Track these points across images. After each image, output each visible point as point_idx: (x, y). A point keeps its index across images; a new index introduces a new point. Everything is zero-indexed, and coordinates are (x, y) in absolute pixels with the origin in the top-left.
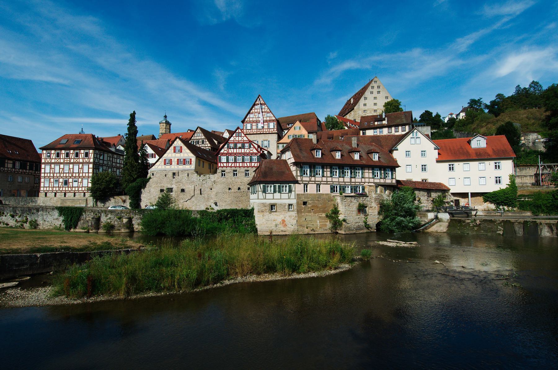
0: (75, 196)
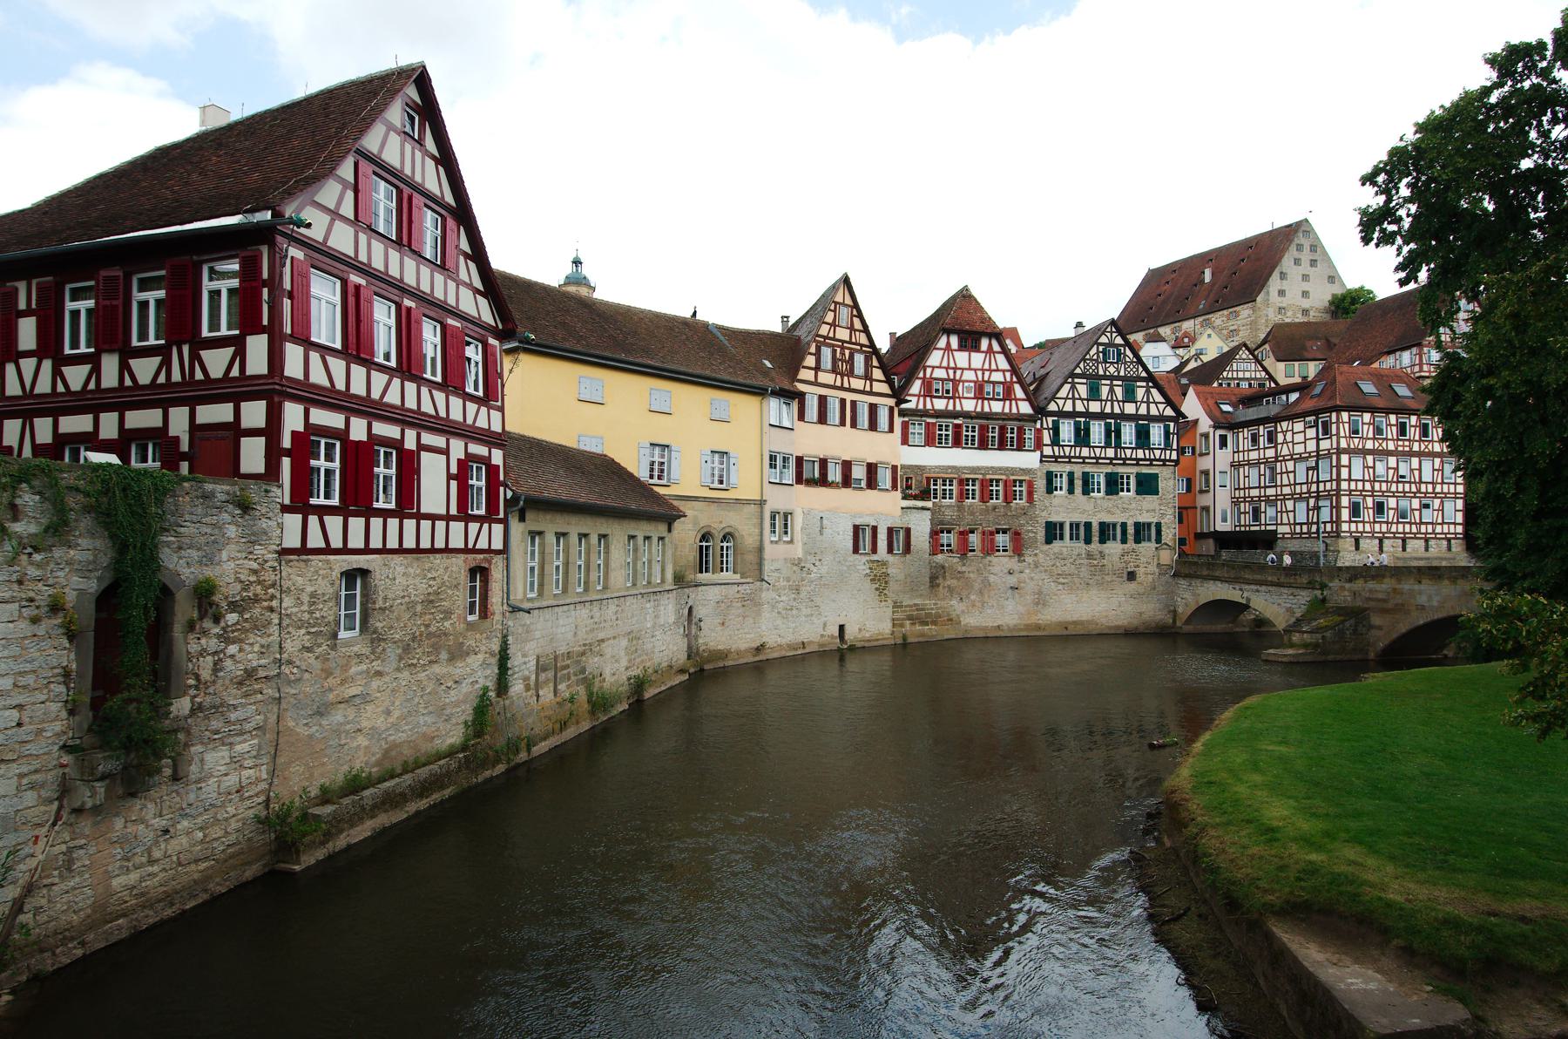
0: (1427, 549)
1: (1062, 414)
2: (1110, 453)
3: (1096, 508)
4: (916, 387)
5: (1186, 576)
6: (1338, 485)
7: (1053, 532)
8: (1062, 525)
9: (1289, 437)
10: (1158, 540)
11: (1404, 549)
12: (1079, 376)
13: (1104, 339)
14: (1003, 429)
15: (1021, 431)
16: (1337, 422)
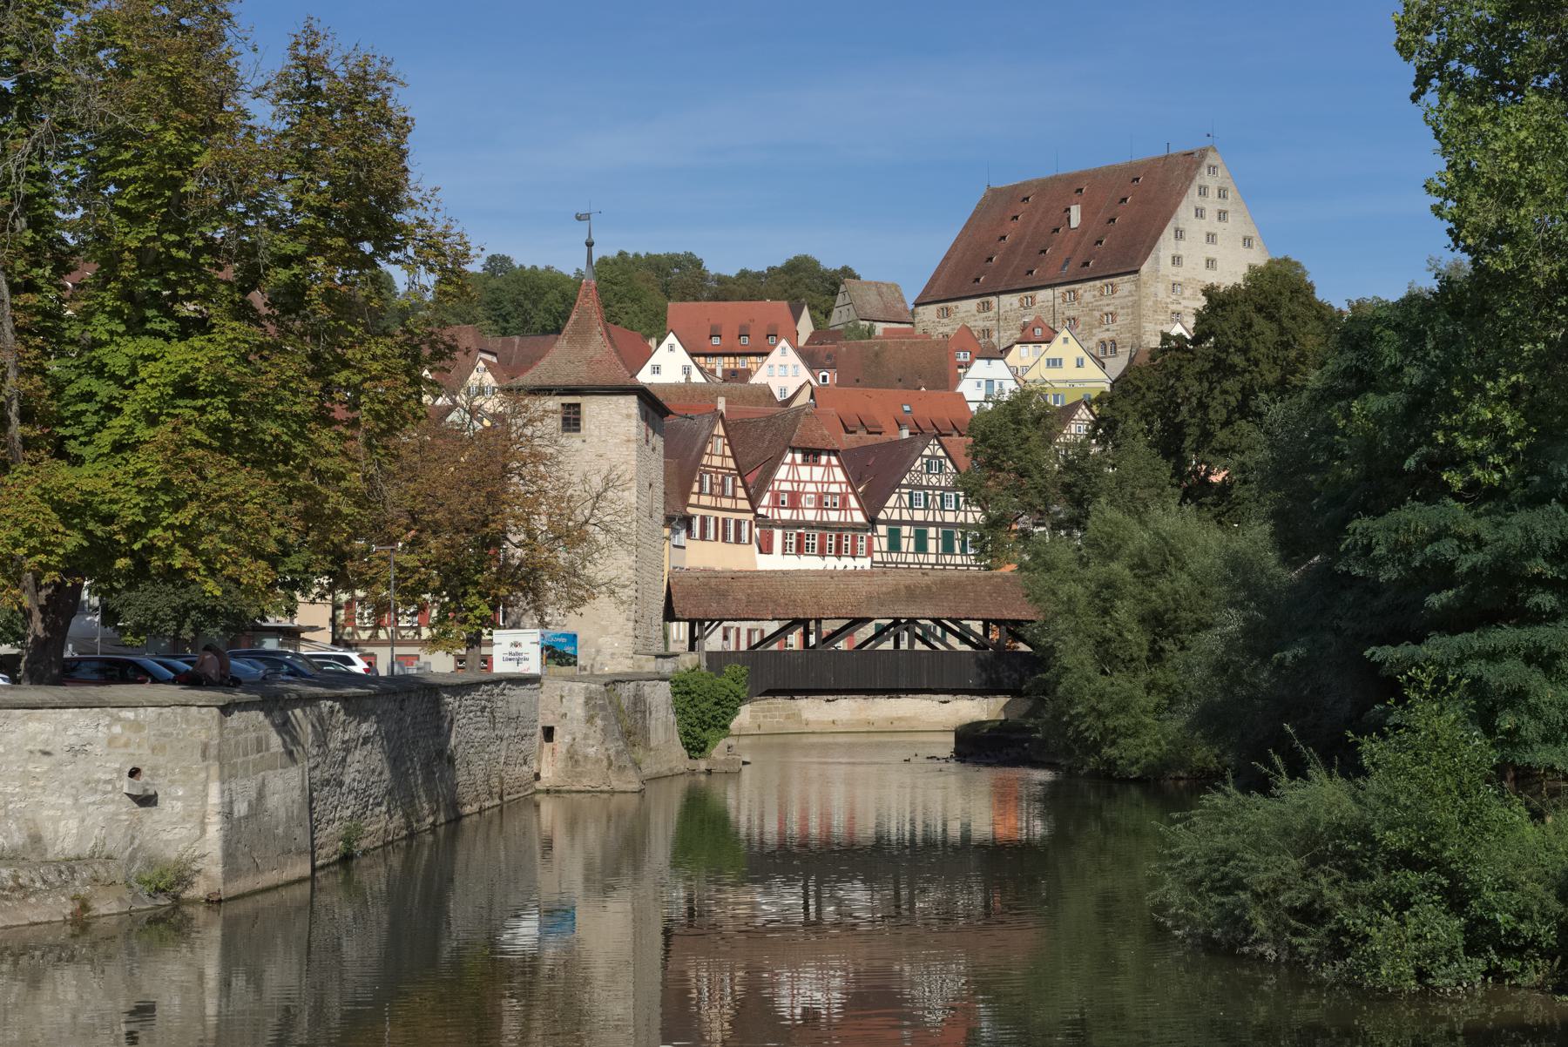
1: (887, 522)
12: (905, 486)
14: (839, 537)
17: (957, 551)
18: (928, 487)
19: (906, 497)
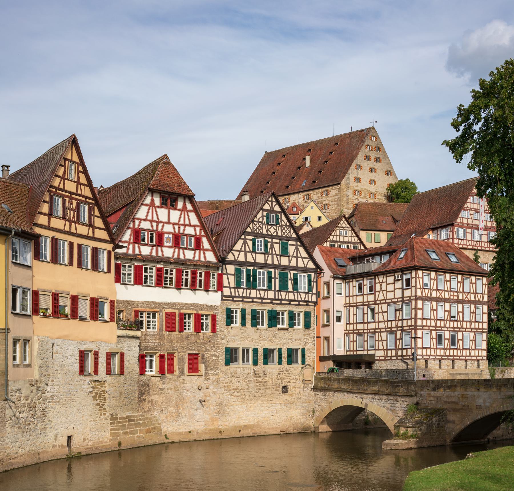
1: (235, 263)
2: (271, 295)
3: (261, 337)
4: (127, 236)
5: (322, 390)
6: (416, 322)
7: (230, 355)
8: (236, 350)
9: (384, 288)
10: (303, 362)
11: (453, 368)
12: (249, 234)
13: (267, 207)
14: (194, 273)
15: (207, 275)
16: (416, 277)
17: (291, 289)
18: (267, 236)
19: (250, 243)
